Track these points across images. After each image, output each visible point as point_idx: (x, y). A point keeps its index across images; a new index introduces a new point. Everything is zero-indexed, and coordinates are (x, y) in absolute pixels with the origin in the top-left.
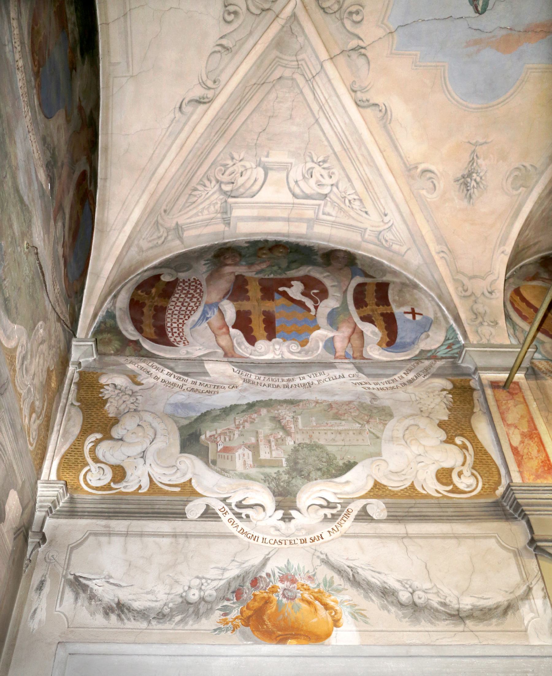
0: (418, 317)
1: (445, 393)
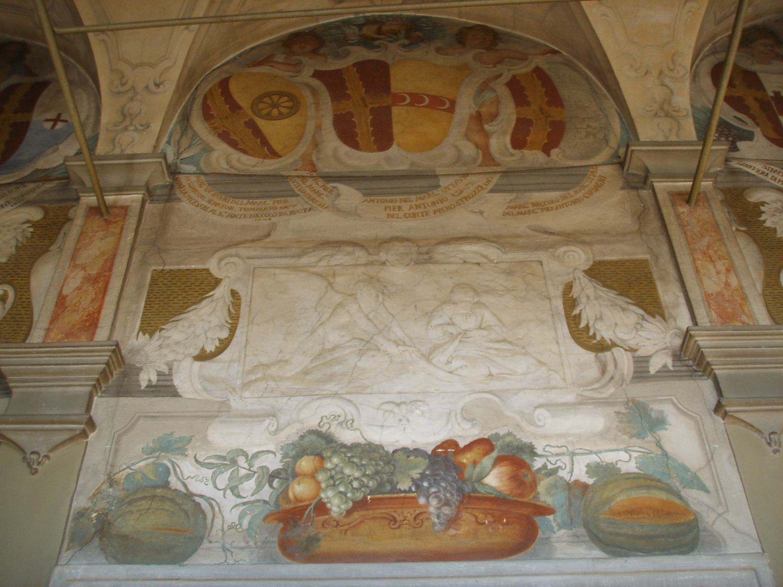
0: (60, 125)
1: (28, 225)
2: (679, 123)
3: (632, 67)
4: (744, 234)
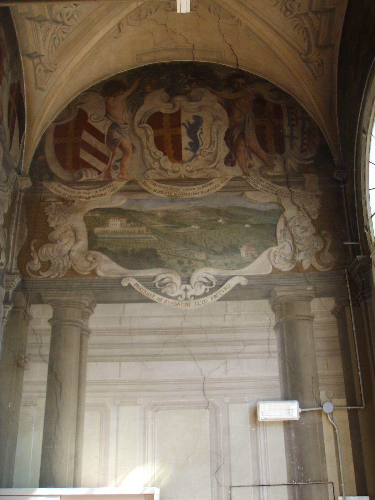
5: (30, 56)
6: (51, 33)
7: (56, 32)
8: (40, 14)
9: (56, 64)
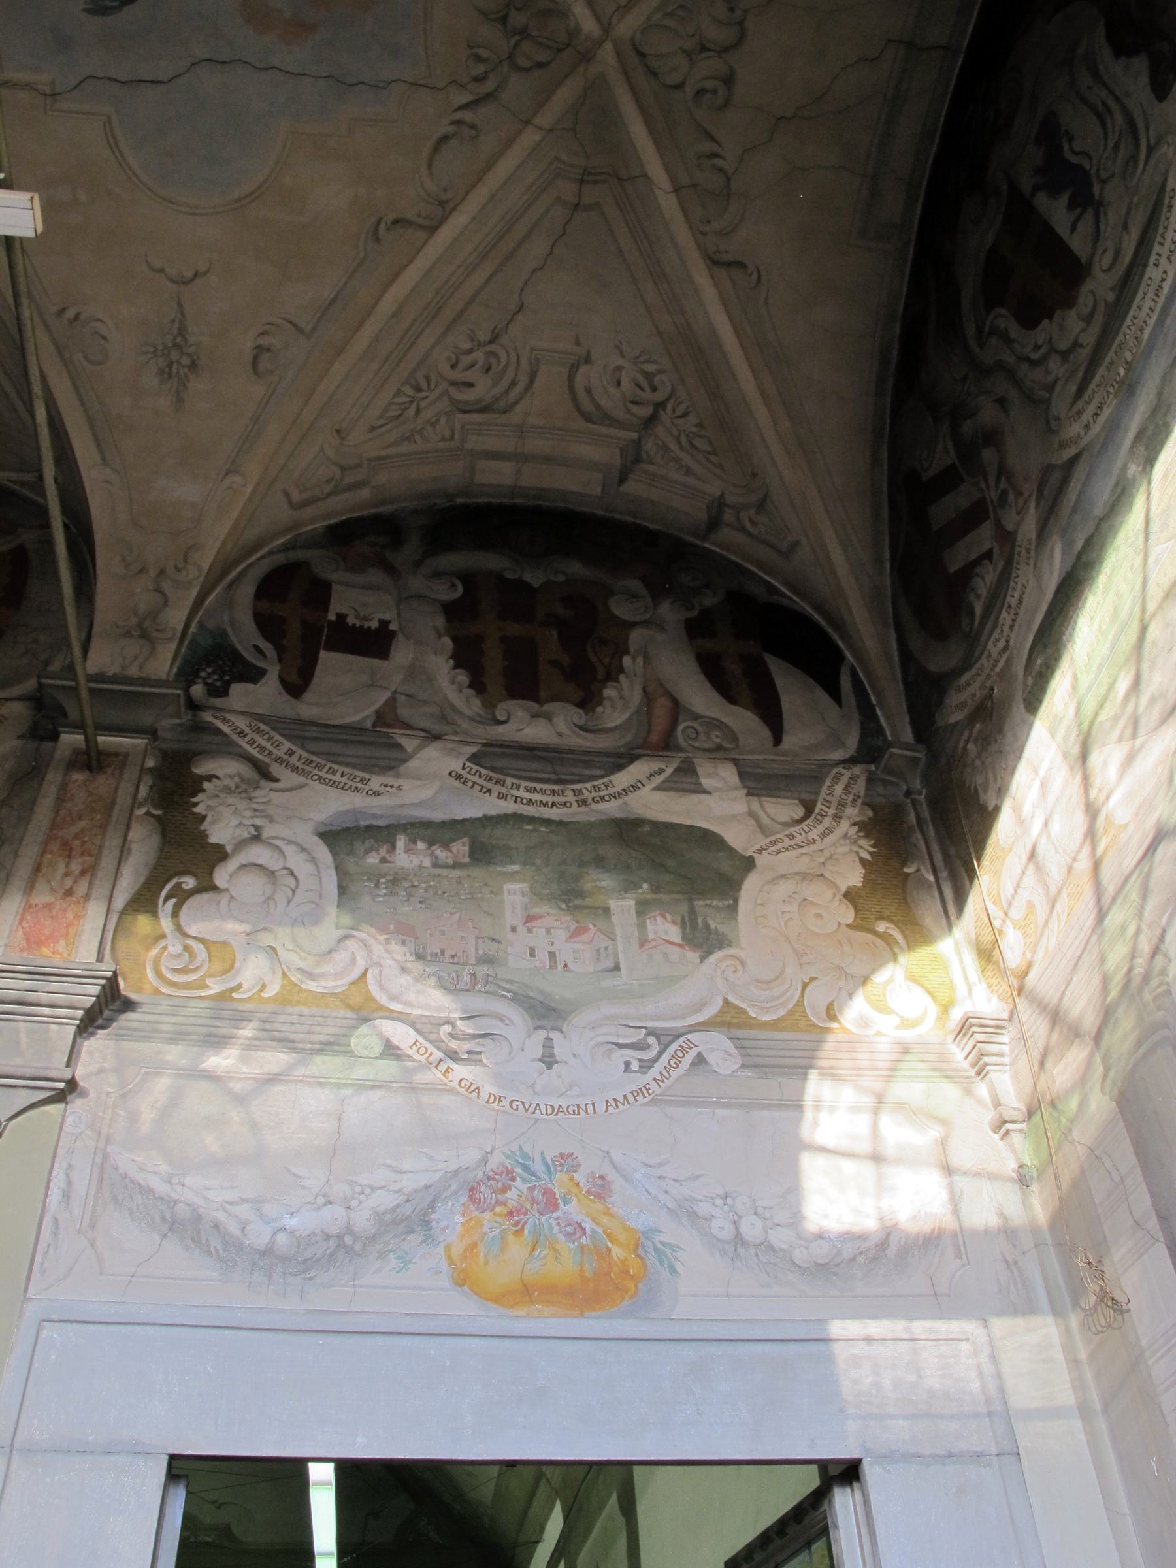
2: (153, 650)
3: (124, 560)
4: (152, 820)
5: (714, 524)
6: (673, 446)
7: (675, 433)
8: (618, 452)
9: (754, 475)
